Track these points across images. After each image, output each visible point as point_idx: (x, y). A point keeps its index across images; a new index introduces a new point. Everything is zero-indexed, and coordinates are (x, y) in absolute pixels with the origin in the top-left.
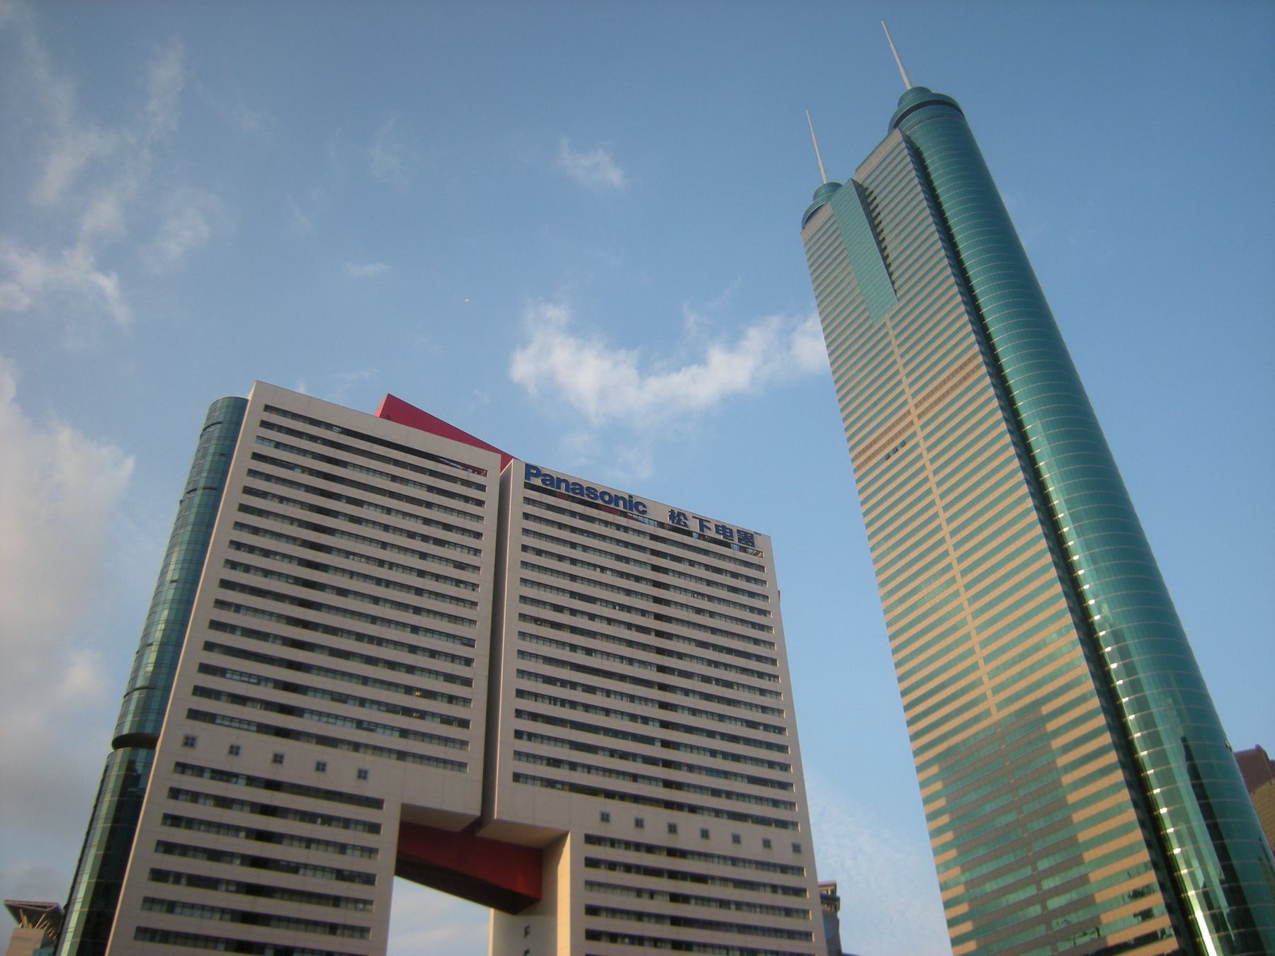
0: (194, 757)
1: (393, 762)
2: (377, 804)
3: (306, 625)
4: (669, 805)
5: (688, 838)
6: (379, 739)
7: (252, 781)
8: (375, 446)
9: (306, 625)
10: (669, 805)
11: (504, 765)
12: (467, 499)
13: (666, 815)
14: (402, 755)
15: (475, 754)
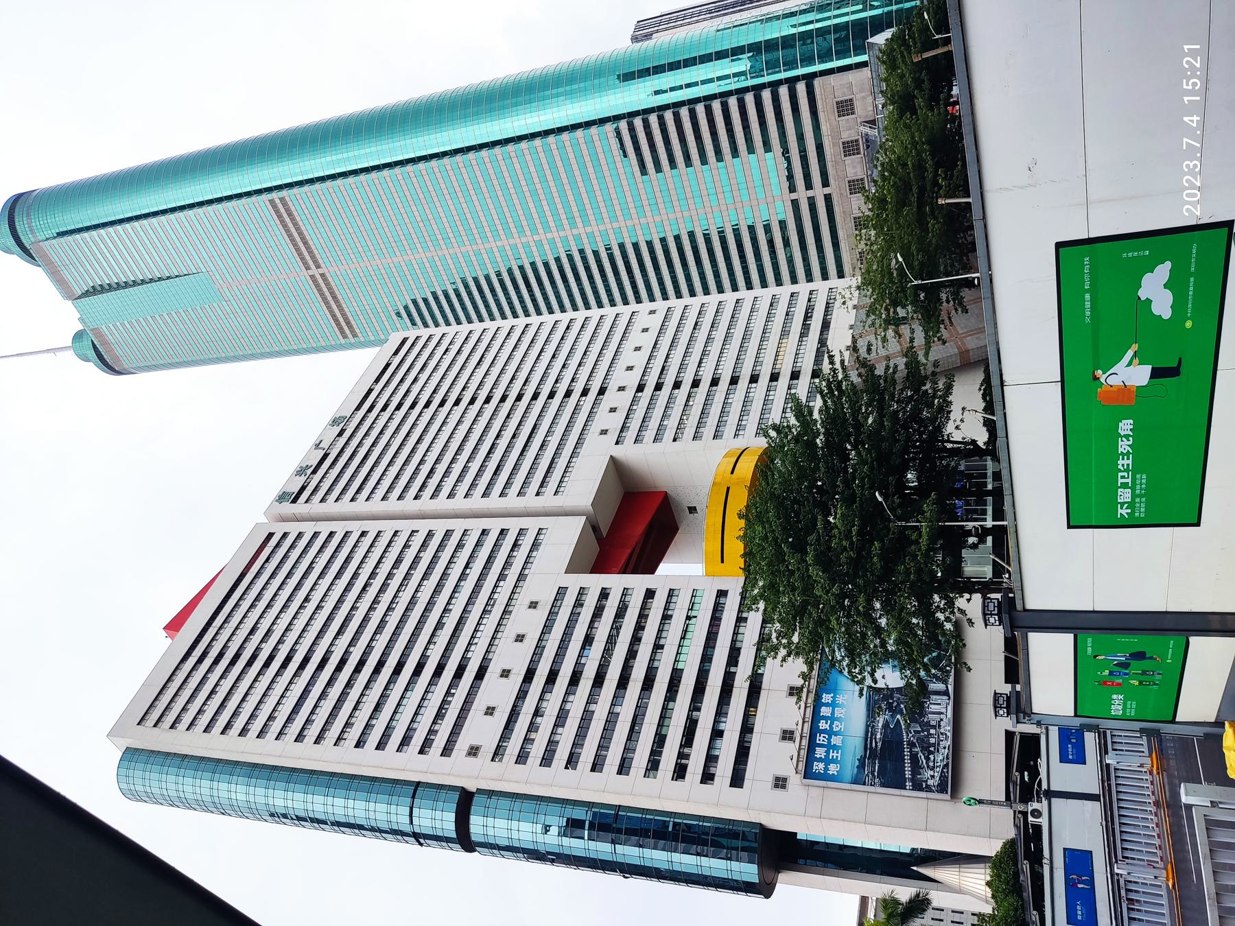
0: (489, 744)
1: (526, 584)
2: (561, 592)
3: (381, 664)
4: (602, 391)
5: (633, 380)
6: (502, 598)
7: (522, 695)
8: (214, 625)
9: (381, 664)
10: (602, 391)
11: (548, 500)
12: (292, 547)
13: (611, 395)
14: (521, 577)
15: (532, 524)
